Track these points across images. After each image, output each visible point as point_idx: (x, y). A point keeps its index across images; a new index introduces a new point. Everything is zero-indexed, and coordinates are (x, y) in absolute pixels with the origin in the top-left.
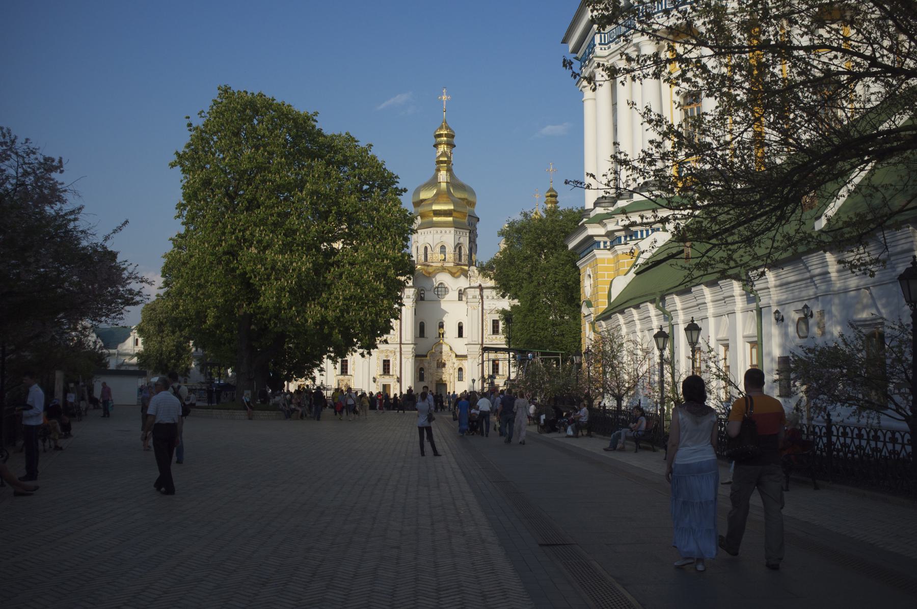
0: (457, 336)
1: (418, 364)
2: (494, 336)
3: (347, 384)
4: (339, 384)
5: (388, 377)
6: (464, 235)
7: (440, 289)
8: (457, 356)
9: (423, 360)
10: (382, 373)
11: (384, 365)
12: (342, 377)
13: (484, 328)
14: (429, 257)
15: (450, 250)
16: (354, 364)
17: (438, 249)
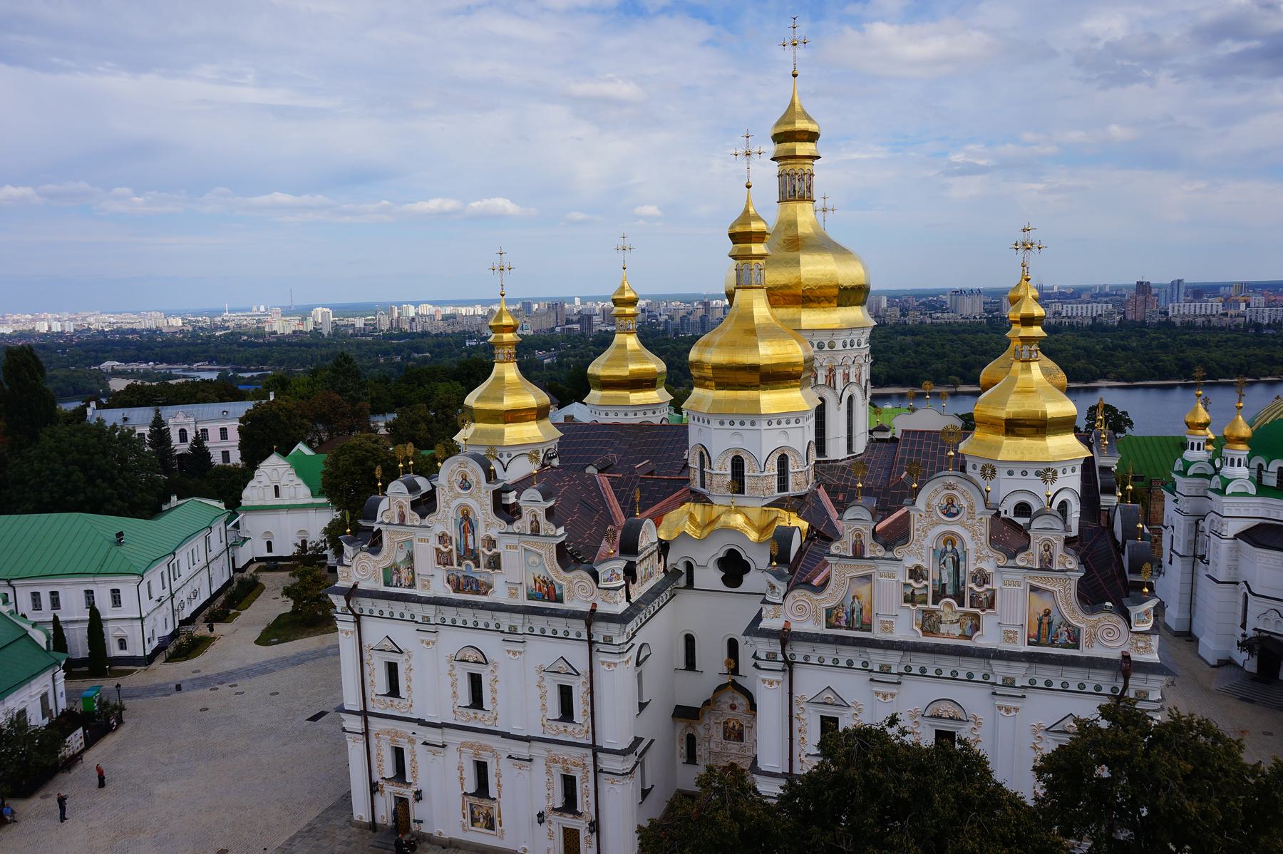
14: (707, 477)
16: (498, 775)
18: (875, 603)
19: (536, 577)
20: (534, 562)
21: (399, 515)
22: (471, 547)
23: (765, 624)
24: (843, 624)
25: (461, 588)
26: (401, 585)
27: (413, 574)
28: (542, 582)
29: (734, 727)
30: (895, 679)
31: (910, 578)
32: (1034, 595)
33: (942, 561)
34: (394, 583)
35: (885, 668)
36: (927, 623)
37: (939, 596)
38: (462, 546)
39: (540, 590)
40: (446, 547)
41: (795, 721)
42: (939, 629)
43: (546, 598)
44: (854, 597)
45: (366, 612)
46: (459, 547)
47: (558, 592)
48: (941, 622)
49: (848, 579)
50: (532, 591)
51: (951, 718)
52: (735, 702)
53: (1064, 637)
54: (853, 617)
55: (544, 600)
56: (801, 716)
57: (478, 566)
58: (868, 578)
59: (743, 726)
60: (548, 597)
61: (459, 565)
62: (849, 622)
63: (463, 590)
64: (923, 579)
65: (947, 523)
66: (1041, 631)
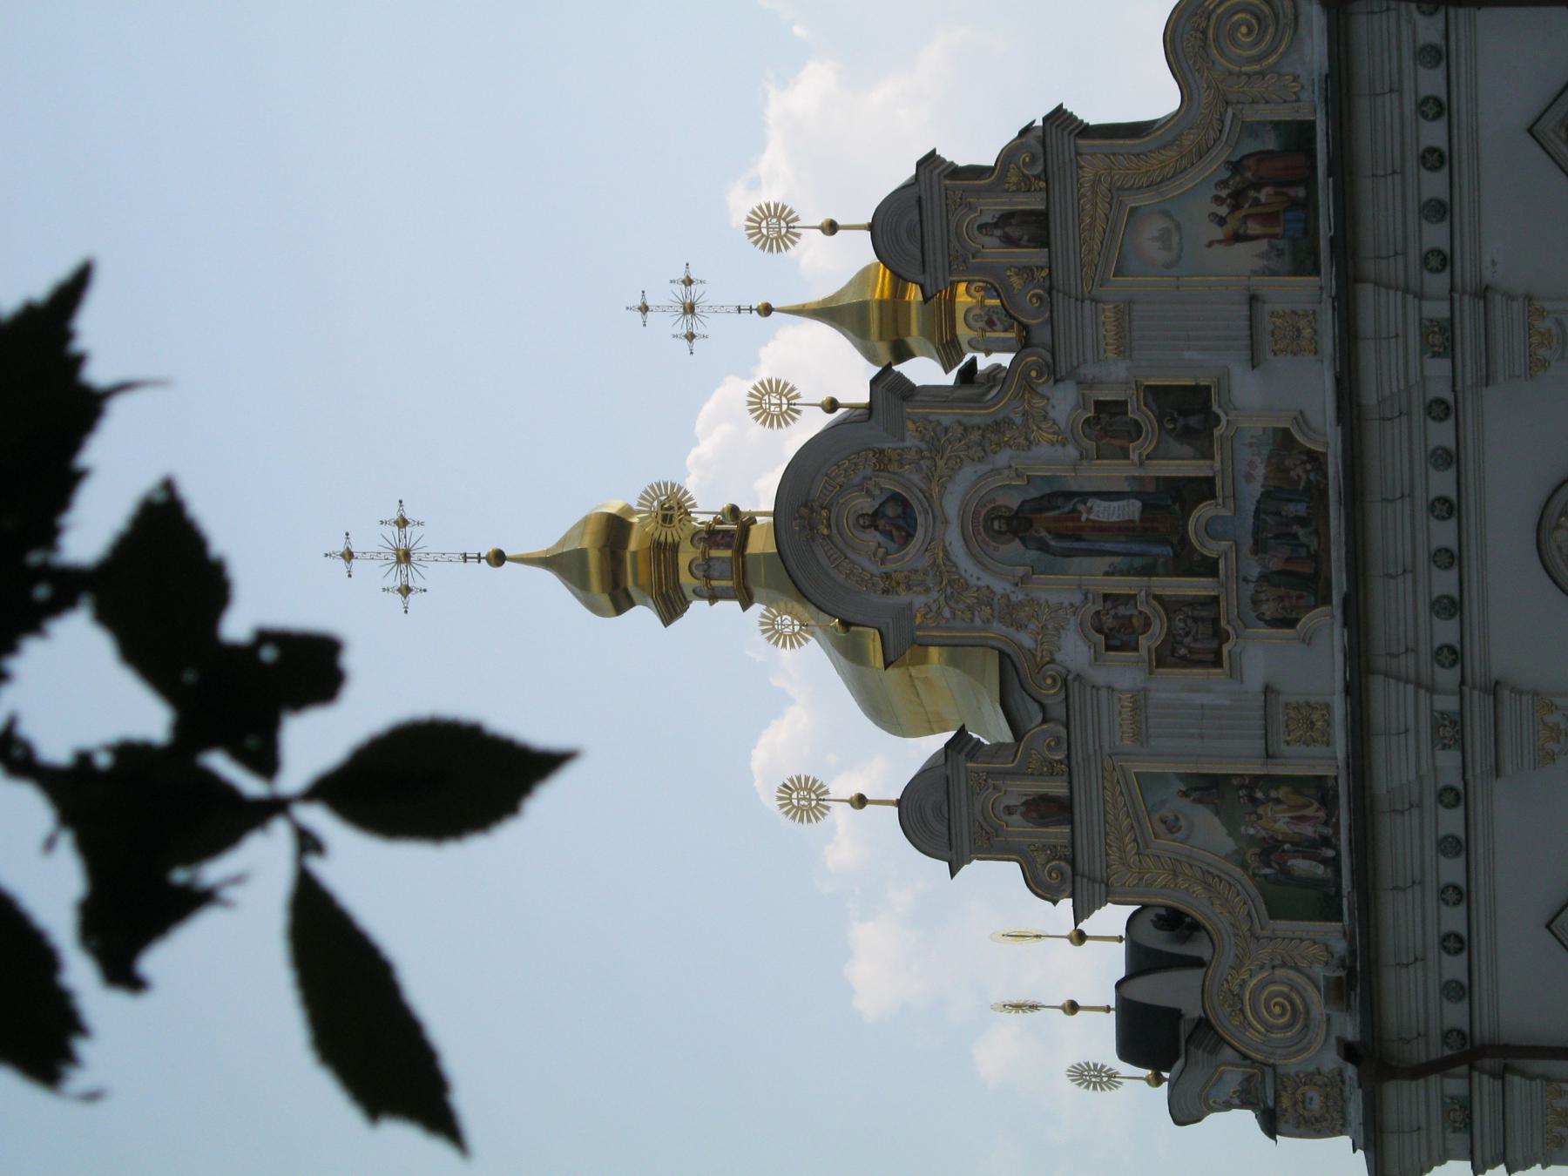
19: (1218, 233)
22: (1129, 510)
25: (1307, 568)
27: (1274, 781)
34: (1320, 870)
38: (1135, 548)
39: (1269, 218)
40: (1147, 624)
43: (1301, 192)
45: (1455, 1016)
47: (1270, 143)
50: (1280, 253)
55: (1308, 205)
57: (1203, 489)
61: (1209, 568)
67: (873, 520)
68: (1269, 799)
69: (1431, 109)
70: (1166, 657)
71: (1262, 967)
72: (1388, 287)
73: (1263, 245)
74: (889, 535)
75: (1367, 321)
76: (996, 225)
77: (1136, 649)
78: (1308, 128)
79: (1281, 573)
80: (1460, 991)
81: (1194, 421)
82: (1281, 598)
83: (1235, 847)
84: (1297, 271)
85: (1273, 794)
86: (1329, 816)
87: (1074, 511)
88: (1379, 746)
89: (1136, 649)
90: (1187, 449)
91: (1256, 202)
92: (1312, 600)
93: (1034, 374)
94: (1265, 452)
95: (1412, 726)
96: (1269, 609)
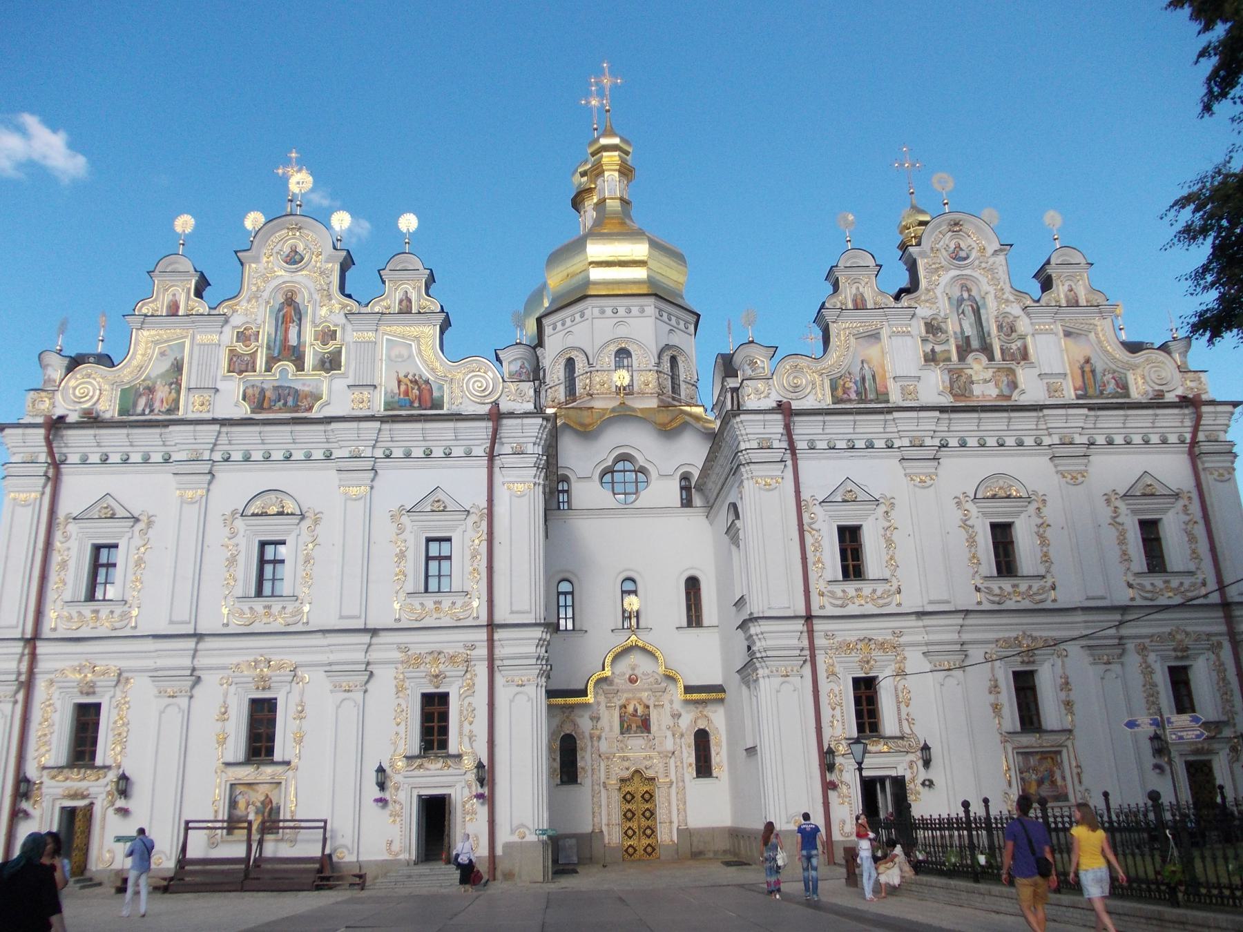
0: (685, 623)
1: (556, 721)
2: (851, 587)
3: (267, 801)
4: (233, 804)
5: (440, 765)
6: (682, 326)
7: (618, 477)
8: (688, 689)
9: (572, 707)
10: (416, 751)
11: (426, 717)
12: (246, 773)
13: (811, 558)
15: (644, 358)
16: (301, 714)
17: (608, 359)
18: (889, 367)
19: (401, 376)
20: (400, 356)
21: (169, 307)
22: (293, 341)
23: (751, 402)
24: (853, 396)
25: (266, 405)
26: (152, 411)
27: (178, 392)
28: (411, 382)
29: (636, 711)
30: (930, 453)
31: (927, 332)
32: (1070, 341)
33: (960, 311)
34: (139, 409)
35: (917, 443)
36: (955, 385)
37: (966, 351)
38: (278, 343)
39: (407, 393)
40: (246, 346)
41: (806, 534)
42: (971, 391)
43: (416, 405)
44: (862, 362)
46: (272, 344)
47: (436, 394)
48: (972, 383)
49: (852, 339)
51: (1008, 497)
52: (638, 672)
53: (1111, 386)
54: (865, 386)
55: (412, 407)
56: (813, 526)
58: (874, 336)
59: (648, 707)
60: (420, 403)
61: (268, 369)
62: (861, 393)
63: (270, 408)
64: (942, 333)
65: (959, 267)
66: (1086, 382)
67: (294, 251)
68: (171, 390)
69: (447, 451)
70: (233, 354)
71: (100, 386)
72: (378, 434)
73: (396, 391)
74: (288, 256)
75: (364, 425)
76: (407, 297)
77: (237, 342)
78: (442, 408)
79: (264, 396)
80: (84, 461)
81: (327, 365)
82: (254, 395)
83: (152, 376)
84: (386, 404)
85: (173, 391)
86: (162, 412)
87: (294, 321)
88: (191, 428)
89: (237, 342)
90: (316, 362)
91: (413, 389)
92: (252, 407)
93: (349, 308)
94: (314, 391)
95: (197, 441)
96: (250, 391)
